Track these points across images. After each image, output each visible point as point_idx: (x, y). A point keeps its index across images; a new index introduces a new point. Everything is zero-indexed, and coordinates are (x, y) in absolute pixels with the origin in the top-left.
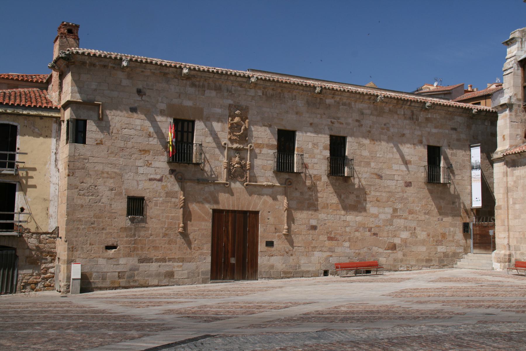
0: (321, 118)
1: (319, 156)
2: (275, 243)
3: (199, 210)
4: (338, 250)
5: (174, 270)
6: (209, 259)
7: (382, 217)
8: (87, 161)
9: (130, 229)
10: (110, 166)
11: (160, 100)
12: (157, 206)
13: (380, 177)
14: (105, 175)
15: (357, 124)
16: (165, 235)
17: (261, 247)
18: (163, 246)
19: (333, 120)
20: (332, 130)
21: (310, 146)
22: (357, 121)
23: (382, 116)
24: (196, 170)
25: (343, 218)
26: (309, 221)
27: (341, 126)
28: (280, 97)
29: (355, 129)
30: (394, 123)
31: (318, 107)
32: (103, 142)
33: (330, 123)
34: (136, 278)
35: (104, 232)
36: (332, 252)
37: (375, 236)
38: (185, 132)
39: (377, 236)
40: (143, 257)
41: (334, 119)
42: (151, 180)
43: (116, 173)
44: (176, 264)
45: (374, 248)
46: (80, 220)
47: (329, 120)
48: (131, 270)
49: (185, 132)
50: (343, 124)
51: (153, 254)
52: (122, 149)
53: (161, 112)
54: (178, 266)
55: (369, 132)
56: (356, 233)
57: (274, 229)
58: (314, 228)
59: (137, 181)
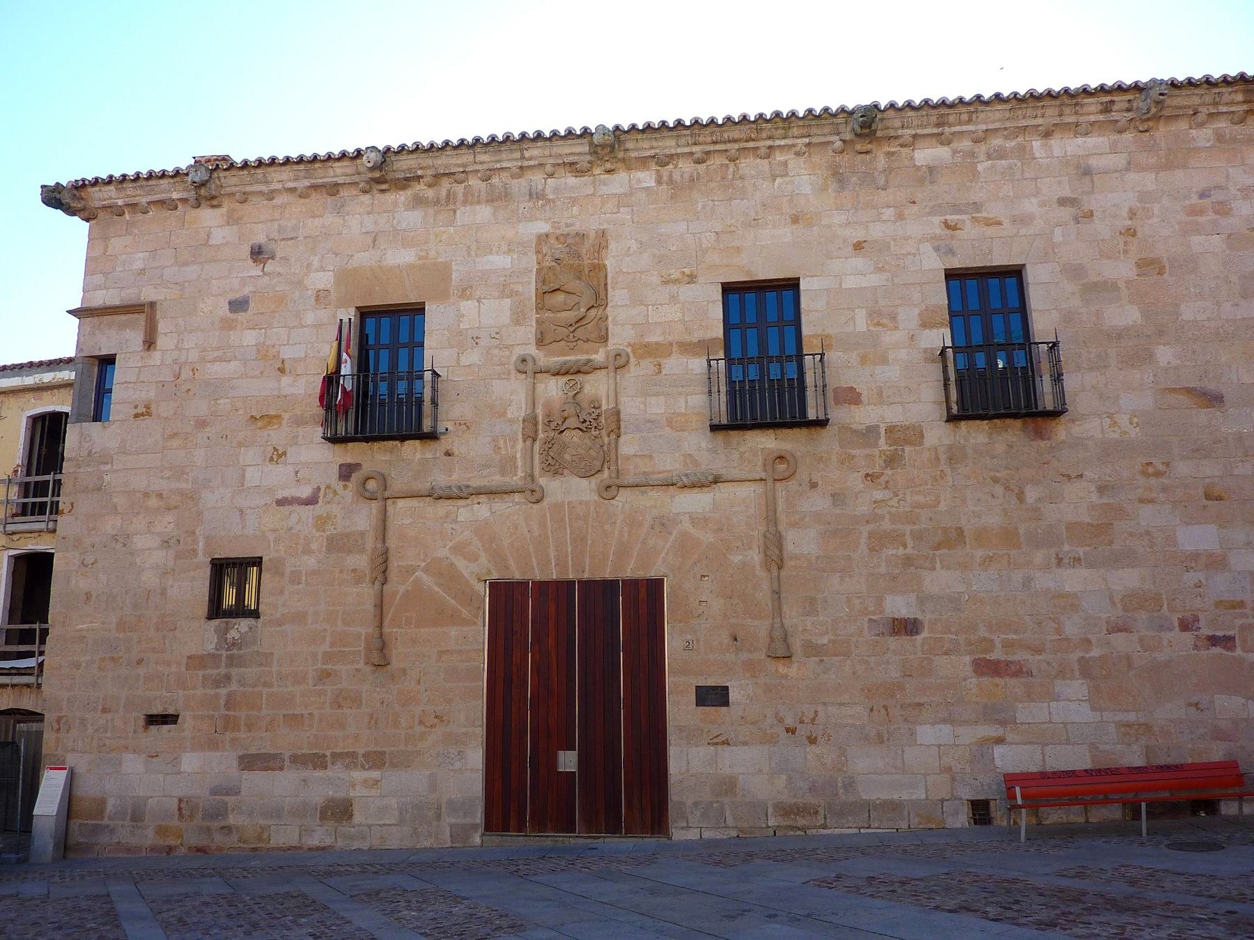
0: (900, 217)
1: (903, 354)
2: (733, 696)
3: (437, 589)
4: (1030, 713)
6: (476, 757)
8: (108, 467)
10: (167, 474)
11: (316, 264)
13: (1213, 399)
14: (153, 502)
15: (1067, 213)
16: (325, 676)
17: (680, 709)
18: (316, 713)
20: (951, 252)
21: (861, 323)
22: (1062, 202)
23: (1185, 167)
24: (429, 455)
25: (1044, 581)
27: (991, 231)
29: (1058, 232)
31: (882, 182)
32: (153, 409)
33: (939, 231)
35: (142, 671)
36: (1003, 723)
37: (1217, 650)
39: (1232, 648)
40: (253, 751)
41: (957, 209)
42: (282, 502)
43: (181, 493)
44: (358, 775)
47: (937, 220)
48: (214, 792)
50: (1000, 223)
51: (285, 741)
52: (202, 424)
56: (1119, 640)
58: (907, 627)
59: (241, 511)
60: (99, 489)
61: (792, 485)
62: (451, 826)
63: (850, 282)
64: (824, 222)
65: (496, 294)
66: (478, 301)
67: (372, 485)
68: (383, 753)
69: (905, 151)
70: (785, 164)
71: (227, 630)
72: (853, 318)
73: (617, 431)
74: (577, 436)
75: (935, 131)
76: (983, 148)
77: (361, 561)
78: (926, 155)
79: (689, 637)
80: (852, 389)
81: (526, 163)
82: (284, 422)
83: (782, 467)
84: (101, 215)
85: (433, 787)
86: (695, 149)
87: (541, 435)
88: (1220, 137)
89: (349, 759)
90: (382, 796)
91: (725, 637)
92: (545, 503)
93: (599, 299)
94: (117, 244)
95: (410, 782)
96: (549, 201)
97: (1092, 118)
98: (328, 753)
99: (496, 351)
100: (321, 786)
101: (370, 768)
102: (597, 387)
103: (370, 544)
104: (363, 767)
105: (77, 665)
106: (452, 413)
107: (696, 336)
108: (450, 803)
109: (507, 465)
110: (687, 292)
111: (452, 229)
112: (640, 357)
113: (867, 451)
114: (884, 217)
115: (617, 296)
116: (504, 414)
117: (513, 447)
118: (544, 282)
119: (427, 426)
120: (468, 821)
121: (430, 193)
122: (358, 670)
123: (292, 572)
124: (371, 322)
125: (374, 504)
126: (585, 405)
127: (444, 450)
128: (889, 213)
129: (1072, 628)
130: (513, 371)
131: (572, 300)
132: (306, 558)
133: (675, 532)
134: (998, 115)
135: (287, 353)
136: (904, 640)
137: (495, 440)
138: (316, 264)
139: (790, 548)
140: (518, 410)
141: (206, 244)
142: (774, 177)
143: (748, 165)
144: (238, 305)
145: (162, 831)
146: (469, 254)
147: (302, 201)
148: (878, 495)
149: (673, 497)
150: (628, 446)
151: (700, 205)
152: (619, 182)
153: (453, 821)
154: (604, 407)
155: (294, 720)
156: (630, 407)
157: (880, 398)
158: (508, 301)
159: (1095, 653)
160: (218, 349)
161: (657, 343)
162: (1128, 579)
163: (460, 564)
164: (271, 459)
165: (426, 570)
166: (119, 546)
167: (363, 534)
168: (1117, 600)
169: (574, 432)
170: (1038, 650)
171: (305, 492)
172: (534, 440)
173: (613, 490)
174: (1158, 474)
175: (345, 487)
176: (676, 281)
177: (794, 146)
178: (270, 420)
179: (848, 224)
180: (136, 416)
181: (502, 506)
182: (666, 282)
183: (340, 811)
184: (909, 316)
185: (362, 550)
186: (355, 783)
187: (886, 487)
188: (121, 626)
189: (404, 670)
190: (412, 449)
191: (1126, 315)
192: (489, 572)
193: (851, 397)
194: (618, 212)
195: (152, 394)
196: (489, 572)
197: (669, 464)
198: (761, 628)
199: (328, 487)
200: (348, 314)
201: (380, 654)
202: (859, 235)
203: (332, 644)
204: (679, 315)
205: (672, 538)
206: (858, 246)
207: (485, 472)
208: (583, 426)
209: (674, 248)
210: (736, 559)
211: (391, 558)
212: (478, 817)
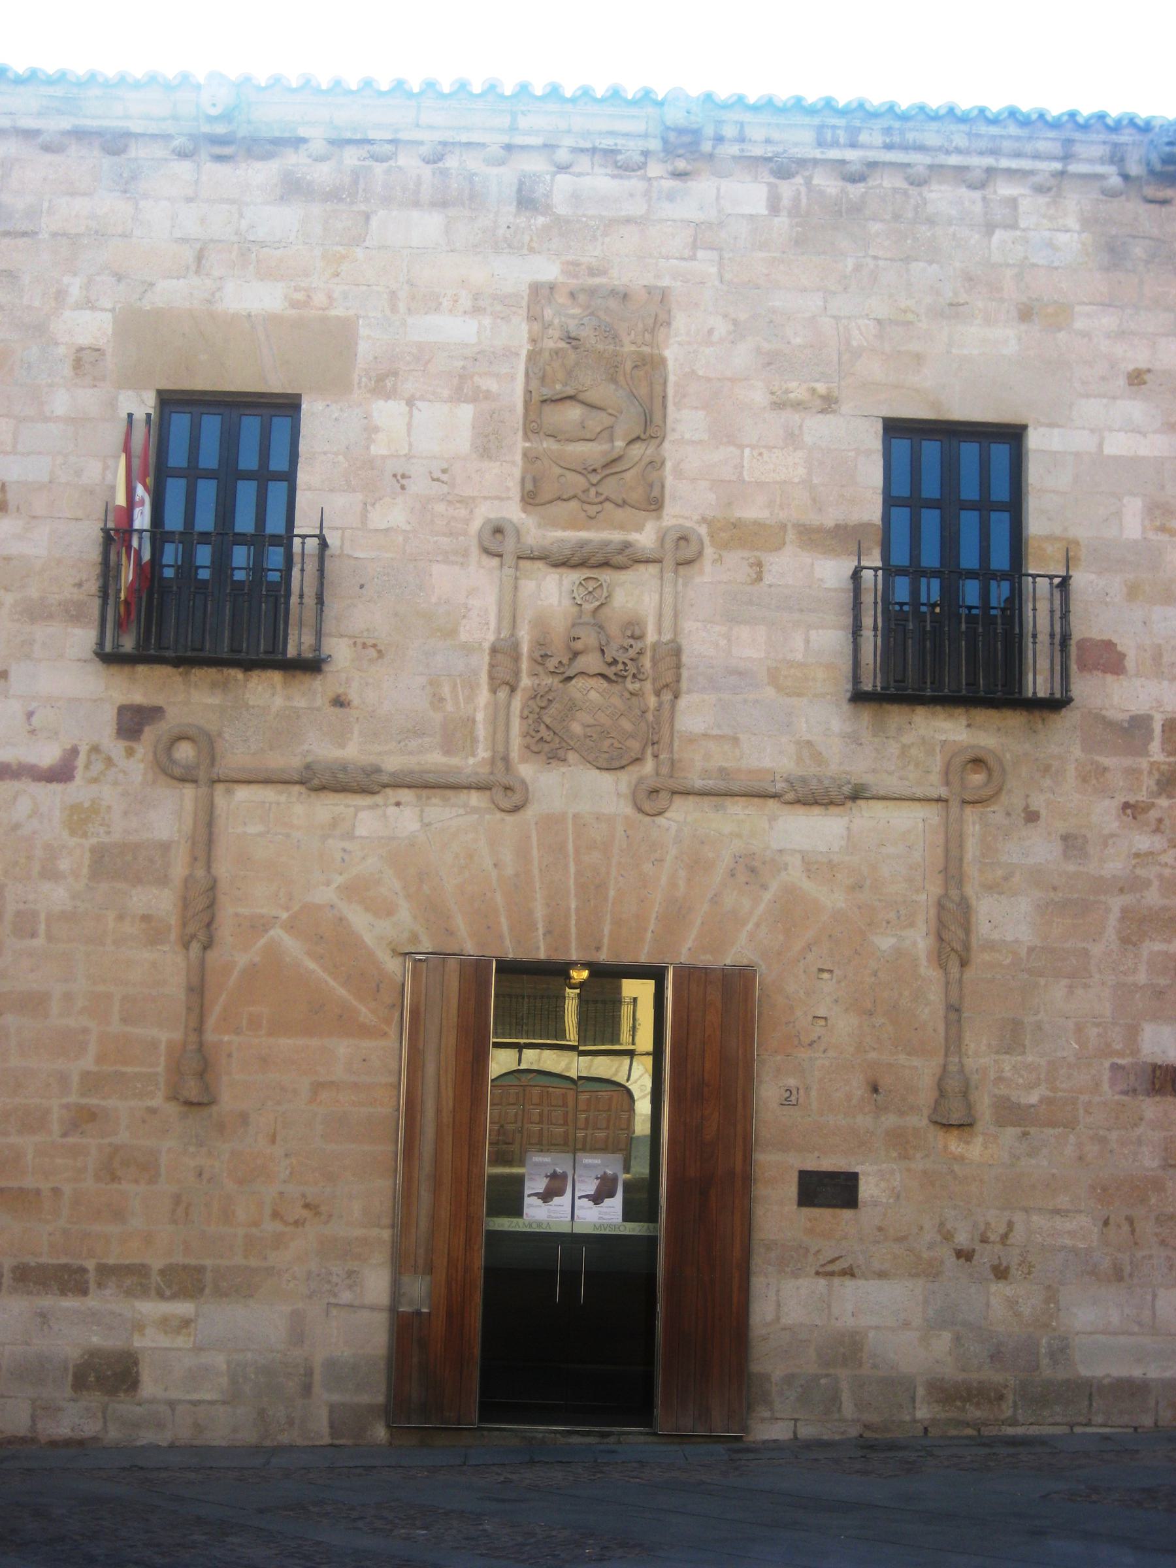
2: (867, 1189)
3: (312, 965)
5: (138, 1342)
18: (67, 1189)
21: (1132, 523)
24: (300, 702)
26: (1133, 1033)
38: (248, 476)
44: (151, 1308)
49: (248, 476)
53: (78, 364)
54: (164, 1323)
61: (996, 814)
62: (332, 1408)
63: (1118, 445)
65: (446, 393)
66: (410, 403)
68: (200, 1269)
70: (1013, 203)
72: (1118, 514)
74: (596, 690)
77: (161, 901)
79: (792, 1082)
80: (1109, 645)
81: (519, 140)
83: (977, 778)
85: (298, 1333)
87: (526, 681)
89: (131, 1277)
90: (198, 1349)
91: (857, 1087)
92: (530, 813)
93: (650, 427)
98: (90, 1264)
99: (441, 508)
101: (174, 1297)
103: (179, 870)
104: (161, 1295)
106: (354, 622)
107: (831, 517)
108: (331, 1364)
109: (456, 734)
110: (817, 429)
112: (725, 546)
113: (1128, 762)
115: (686, 423)
116: (453, 633)
117: (470, 699)
119: (297, 643)
122: (153, 1111)
123: (18, 914)
124: (180, 423)
125: (189, 791)
126: (614, 629)
127: (331, 695)
130: (475, 551)
131: (597, 421)
132: (46, 887)
133: (774, 886)
137: (434, 683)
138: (75, 291)
139: (983, 928)
140: (481, 627)
142: (990, 228)
146: (394, 309)
147: (48, 157)
148: (1144, 842)
149: (772, 819)
150: (694, 715)
151: (850, 263)
153: (336, 1398)
154: (651, 637)
156: (702, 642)
157: (1156, 663)
158: (466, 413)
161: (756, 523)
163: (359, 920)
167: (165, 847)
169: (592, 682)
171: (47, 755)
172: (513, 689)
175: (130, 752)
176: (798, 405)
177: (1032, 173)
179: (1121, 335)
182: (779, 405)
185: (163, 880)
187: (1157, 830)
189: (244, 1118)
190: (265, 692)
192: (414, 938)
193: (1109, 660)
194: (693, 258)
196: (414, 938)
197: (770, 756)
198: (923, 1073)
199: (95, 749)
200: (143, 404)
201: (195, 1083)
203: (100, 1059)
205: (768, 896)
206: (1137, 378)
207: (413, 744)
208: (610, 672)
209: (798, 341)
210: (885, 943)
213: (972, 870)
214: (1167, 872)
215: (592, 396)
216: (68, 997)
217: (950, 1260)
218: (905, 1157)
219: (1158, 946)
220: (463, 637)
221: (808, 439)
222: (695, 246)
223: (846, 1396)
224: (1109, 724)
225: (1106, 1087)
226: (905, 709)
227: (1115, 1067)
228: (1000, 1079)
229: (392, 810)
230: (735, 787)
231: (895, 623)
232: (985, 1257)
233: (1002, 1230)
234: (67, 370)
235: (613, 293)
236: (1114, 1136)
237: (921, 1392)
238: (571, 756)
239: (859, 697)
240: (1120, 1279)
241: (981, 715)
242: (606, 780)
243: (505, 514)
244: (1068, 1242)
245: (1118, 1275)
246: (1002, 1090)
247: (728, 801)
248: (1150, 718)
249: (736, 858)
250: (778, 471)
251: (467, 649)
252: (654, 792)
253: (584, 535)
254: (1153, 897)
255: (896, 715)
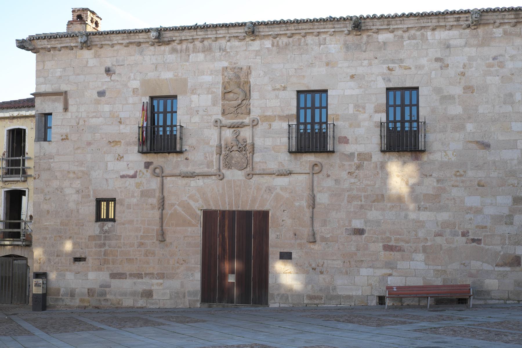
0: (370, 65)
1: (366, 124)
3: (183, 213)
4: (402, 265)
6: (198, 276)
7: (490, 211)
8: (52, 160)
9: (98, 237)
10: (77, 164)
11: (132, 77)
12: (130, 209)
13: (486, 146)
14: (72, 175)
15: (438, 65)
18: (138, 258)
19: (391, 66)
20: (389, 80)
21: (351, 110)
22: (437, 60)
23: (489, 46)
24: (179, 159)
26: (350, 221)
27: (406, 72)
28: (299, 45)
29: (433, 72)
30: (514, 52)
31: (364, 49)
32: (69, 137)
33: (385, 71)
34: (108, 297)
36: (392, 268)
37: (474, 244)
39: (480, 244)
40: (115, 272)
41: (393, 61)
42: (122, 177)
43: (83, 172)
44: (155, 281)
45: (473, 263)
46: (47, 228)
47: (385, 66)
48: (101, 286)
50: (410, 68)
51: (127, 268)
52: (89, 144)
54: (157, 284)
55: (463, 74)
56: (438, 239)
57: (292, 235)
58: (360, 232)
59: (107, 180)
60: (49, 169)
61: (320, 175)
62: (189, 300)
63: (348, 92)
64: (339, 66)
65: (206, 93)
66: (199, 95)
67: (157, 171)
68: (164, 273)
69: (375, 35)
70: (325, 39)
71: (103, 226)
72: (348, 108)
73: (253, 152)
74: (238, 153)
75: (386, 27)
76: (406, 35)
77: (154, 201)
78: (382, 37)
79: (278, 234)
80: (345, 137)
82: (122, 144)
83: (316, 168)
84: (41, 51)
85: (182, 285)
86: (288, 32)
87: (223, 152)
88: (505, 33)
89: (151, 275)
90: (163, 289)
91: (291, 234)
92: (224, 180)
93: (247, 96)
94: (49, 64)
95: (175, 284)
96: (228, 52)
97: (451, 24)
98: (143, 273)
99: (205, 117)
100: (142, 285)
101: (159, 279)
102: (246, 133)
104: (156, 278)
105: (45, 238)
106: (189, 142)
108: (189, 292)
109: (209, 165)
110: (282, 94)
111: (188, 63)
112: (263, 121)
113: (350, 163)
114: (364, 64)
115: (255, 95)
117: (212, 157)
118: (225, 88)
120: (195, 298)
121: (179, 47)
122: (154, 243)
123: (127, 205)
125: (159, 179)
126: (241, 141)
128: (366, 62)
129: (421, 234)
130: (212, 126)
132: (132, 199)
133: (274, 193)
134: (412, 22)
135: (122, 115)
136: (358, 237)
137: (205, 154)
138: (132, 77)
139: (318, 200)
140: (214, 142)
141: (86, 66)
142: (320, 45)
143: (310, 39)
144: (101, 94)
145: (82, 301)
146: (195, 75)
147: (126, 48)
148: (353, 180)
149: (273, 179)
150: (257, 158)
151: (289, 56)
152: (256, 45)
154: (248, 142)
155: (130, 261)
156: (259, 142)
157: (356, 142)
159: (429, 243)
160: (94, 112)
161: (270, 116)
162: (444, 216)
163: (192, 203)
164: (118, 159)
165: (179, 205)
166: (59, 192)
167: (154, 190)
168: (439, 224)
170: (407, 242)
171: (131, 173)
172: (220, 155)
173: (251, 176)
174: (461, 176)
175: (147, 171)
176: (278, 89)
178: (117, 143)
179: (349, 67)
180: (62, 139)
181: (208, 181)
182: (274, 90)
183: (148, 294)
184: (370, 108)
185: (154, 197)
186: (154, 284)
187: (356, 178)
188: (62, 223)
189: (171, 243)
190: (173, 158)
191: (456, 110)
192: (203, 207)
193: (345, 140)
194: (256, 58)
195: (68, 130)
196: (203, 207)
197: (273, 166)
198: (306, 231)
199: (140, 171)
200: (146, 100)
201: (162, 237)
202: (352, 72)
203: (144, 233)
204: (279, 104)
205: (273, 195)
206: (352, 77)
207: (201, 167)
209: (278, 75)
210: (297, 204)
211: (165, 200)
212: (199, 297)
213: (316, 189)
214: (358, 187)
215: (235, 91)
216: (137, 221)
217: (311, 270)
218: (301, 249)
219: (356, 203)
220: (211, 144)
221: (280, 97)
222: (256, 56)
223: (290, 298)
224: (345, 155)
225: (344, 233)
226: (301, 154)
227: (346, 229)
228: (322, 232)
229: (198, 181)
230: (265, 172)
231: (300, 136)
232: (318, 269)
233: (322, 263)
234: (132, 93)
235: (239, 68)
236: (346, 244)
237: (305, 297)
238: (232, 168)
239: (291, 152)
240: (347, 274)
241: (317, 154)
242: (240, 172)
243: (218, 118)
244: (336, 266)
245: (347, 273)
246: (322, 234)
247: (264, 176)
248: (354, 153)
249: (266, 188)
250: (274, 104)
251: (211, 146)
252: (248, 175)
253: (234, 121)
254: (355, 192)
255: (299, 155)
